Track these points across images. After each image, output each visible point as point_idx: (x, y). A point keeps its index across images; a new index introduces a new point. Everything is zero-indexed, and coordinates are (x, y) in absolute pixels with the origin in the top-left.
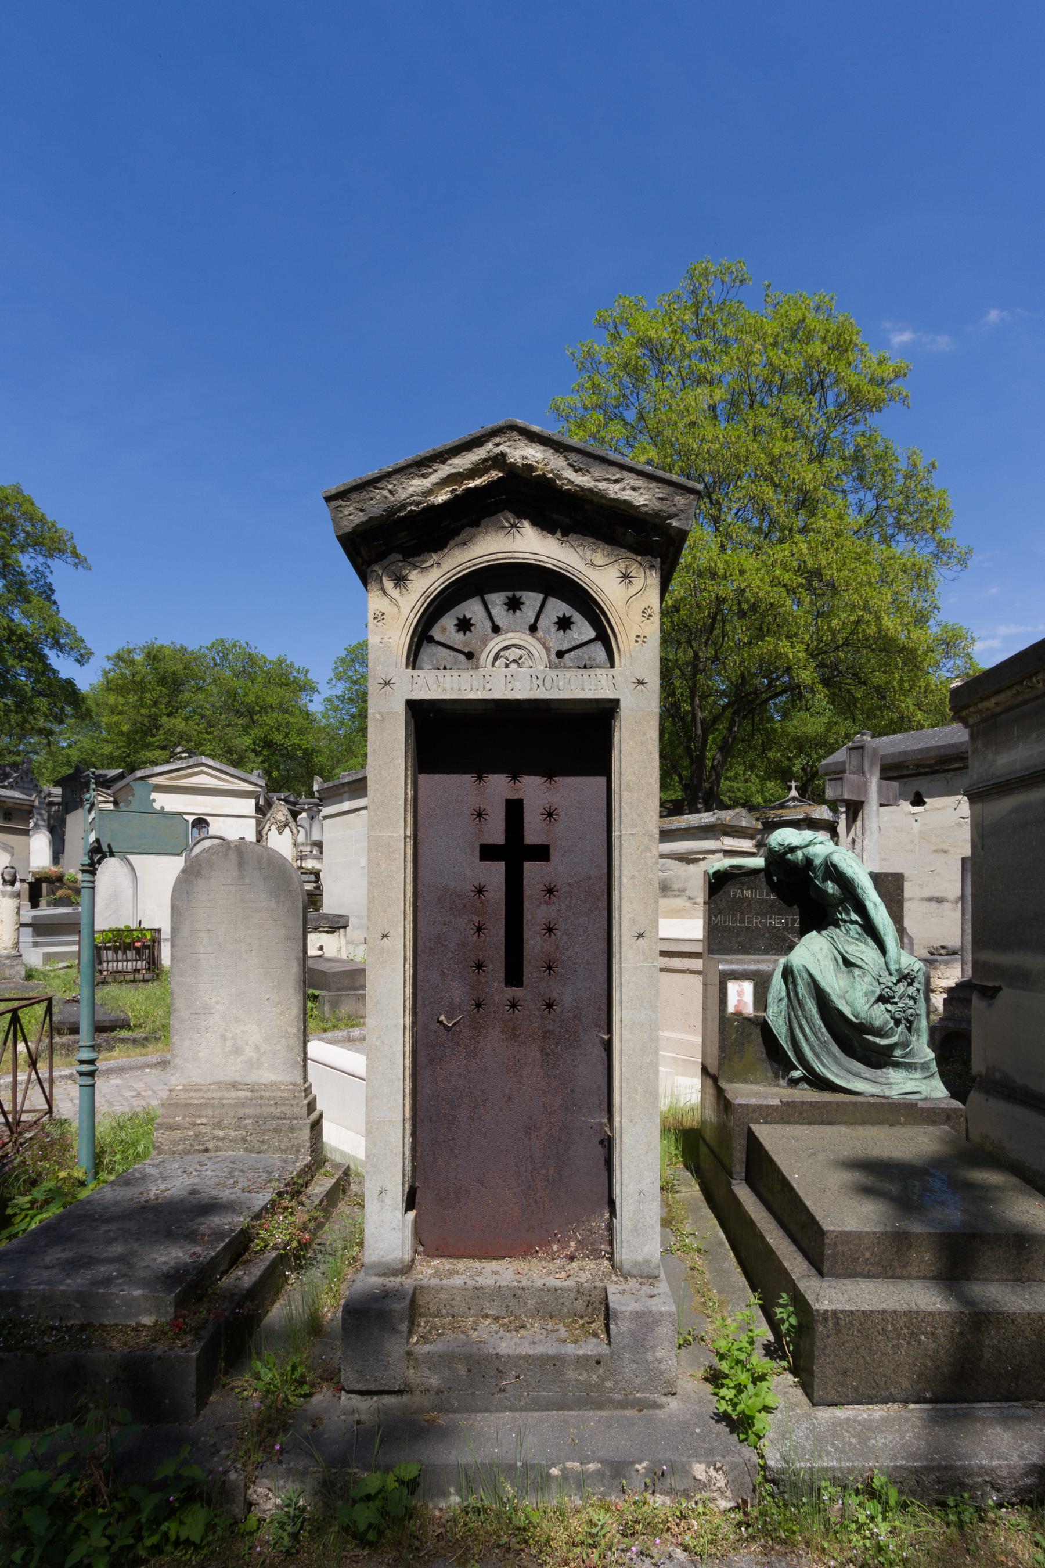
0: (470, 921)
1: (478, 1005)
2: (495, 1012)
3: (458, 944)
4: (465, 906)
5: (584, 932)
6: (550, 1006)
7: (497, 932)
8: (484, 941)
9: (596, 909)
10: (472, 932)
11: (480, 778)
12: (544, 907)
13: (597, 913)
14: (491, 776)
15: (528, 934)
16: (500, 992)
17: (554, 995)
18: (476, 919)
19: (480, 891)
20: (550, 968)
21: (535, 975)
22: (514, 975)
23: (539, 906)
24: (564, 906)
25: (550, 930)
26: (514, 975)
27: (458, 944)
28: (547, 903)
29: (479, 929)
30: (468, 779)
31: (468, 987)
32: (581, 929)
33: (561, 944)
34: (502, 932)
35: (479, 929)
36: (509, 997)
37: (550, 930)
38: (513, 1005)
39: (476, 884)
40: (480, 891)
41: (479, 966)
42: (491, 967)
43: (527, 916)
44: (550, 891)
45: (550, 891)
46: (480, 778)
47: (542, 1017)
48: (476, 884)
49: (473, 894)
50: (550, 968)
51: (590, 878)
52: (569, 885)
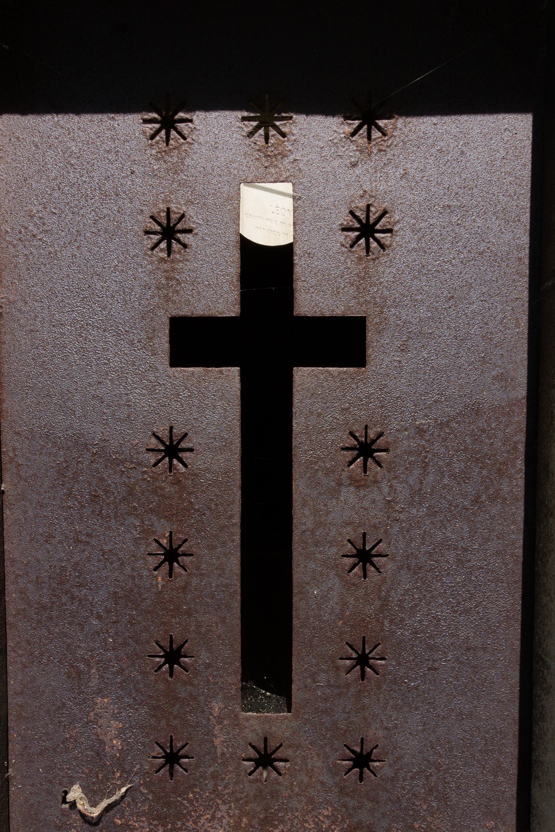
0: (146, 532)
1: (172, 758)
2: (214, 776)
3: (115, 596)
4: (131, 492)
5: (460, 562)
6: (362, 761)
7: (220, 563)
8: (184, 589)
9: (492, 499)
10: (153, 561)
11: (168, 124)
12: (348, 494)
13: (494, 510)
14: (198, 117)
15: (302, 569)
16: (231, 723)
17: (375, 733)
18: (163, 529)
19: (172, 449)
20: (363, 660)
21: (322, 678)
22: (267, 661)
23: (334, 493)
24: (403, 492)
25: (364, 557)
26: (267, 661)
27: (115, 596)
28: (357, 484)
29: (172, 555)
30: (131, 127)
31: (144, 710)
32: (451, 556)
33: (395, 596)
34: (234, 563)
35: (172, 555)
36: (251, 737)
37: (364, 557)
38: (265, 759)
39: (164, 434)
40: (172, 449)
41: (173, 656)
42: (204, 657)
43: (303, 517)
44: (365, 449)
45: (365, 449)
46: (168, 124)
47: (342, 791)
48: (164, 434)
49: (152, 458)
50: (363, 660)
51: (478, 412)
52: (420, 431)
